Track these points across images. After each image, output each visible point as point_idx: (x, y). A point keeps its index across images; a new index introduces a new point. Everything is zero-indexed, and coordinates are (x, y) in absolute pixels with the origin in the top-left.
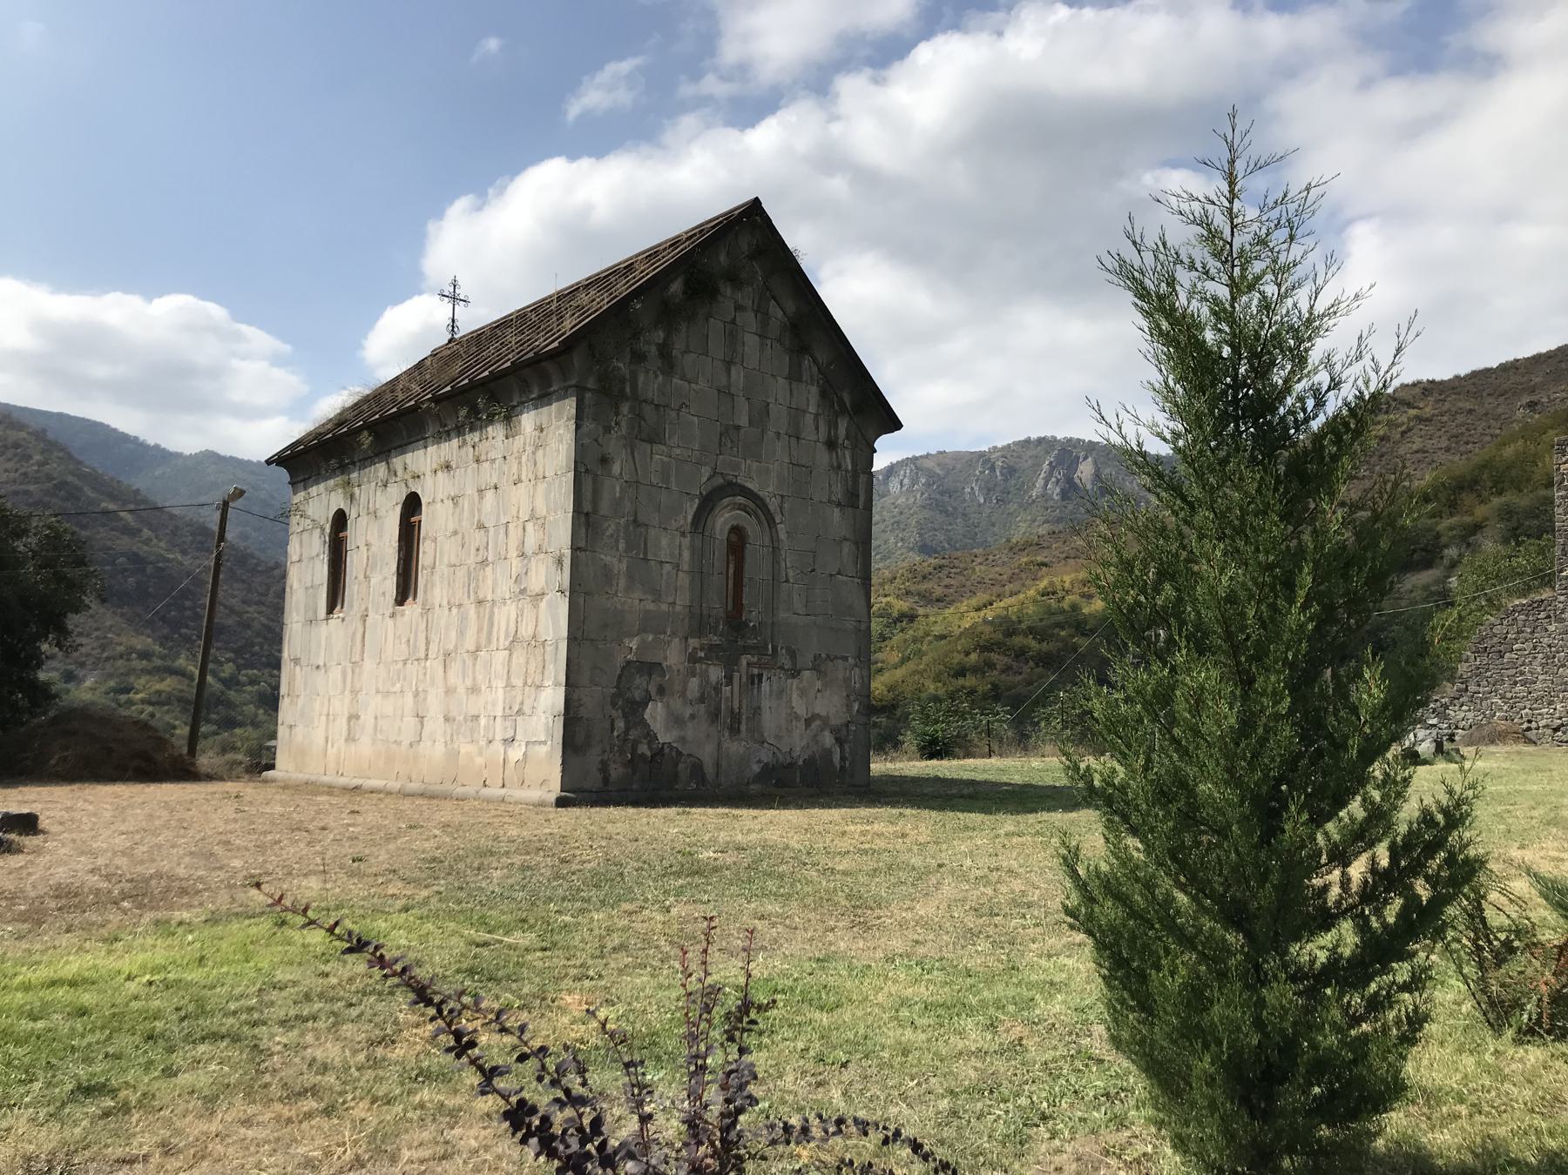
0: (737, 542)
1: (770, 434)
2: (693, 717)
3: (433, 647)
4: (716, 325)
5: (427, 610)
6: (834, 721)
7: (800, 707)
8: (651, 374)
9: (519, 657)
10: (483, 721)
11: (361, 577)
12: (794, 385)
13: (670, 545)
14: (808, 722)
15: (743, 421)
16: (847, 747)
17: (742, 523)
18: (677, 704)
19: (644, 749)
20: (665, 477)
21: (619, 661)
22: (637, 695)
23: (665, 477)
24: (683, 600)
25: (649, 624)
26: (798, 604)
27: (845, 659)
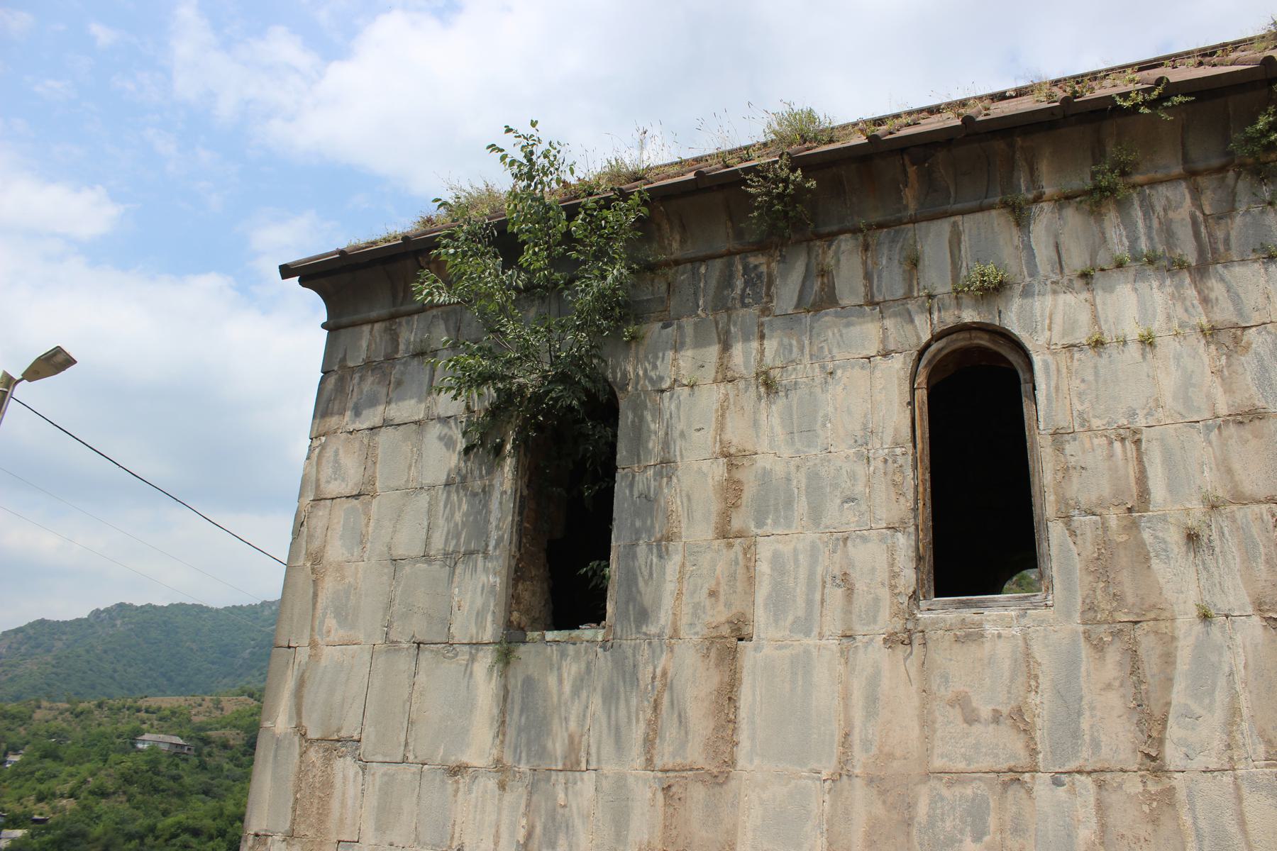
3: (1192, 739)
5: (1125, 627)
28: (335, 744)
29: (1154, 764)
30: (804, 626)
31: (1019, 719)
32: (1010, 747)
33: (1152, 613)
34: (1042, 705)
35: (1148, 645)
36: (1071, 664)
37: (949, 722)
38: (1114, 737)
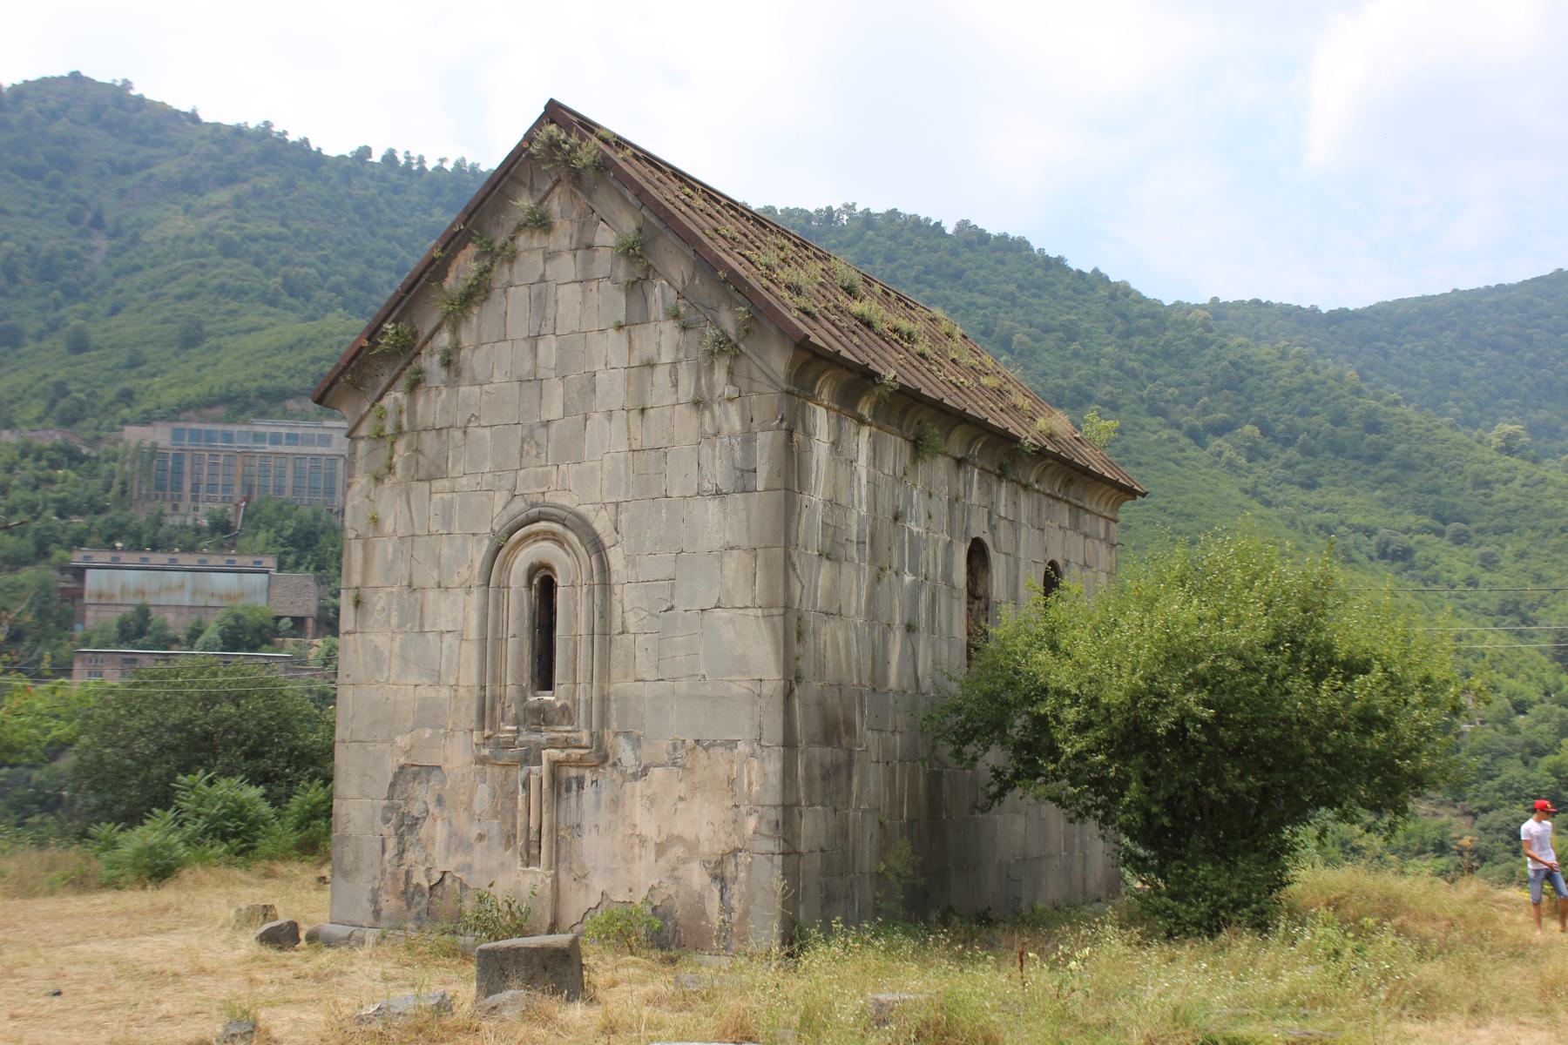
0: (544, 586)
1: (597, 418)
2: (481, 837)
4: (519, 294)
6: (705, 848)
7: (647, 826)
8: (433, 393)
12: (637, 332)
13: (457, 612)
14: (661, 849)
15: (554, 409)
16: (736, 890)
17: (547, 559)
18: (461, 819)
19: (419, 878)
20: (447, 519)
21: (391, 766)
22: (416, 809)
23: (447, 519)
24: (470, 676)
25: (428, 715)
26: (644, 668)
27: (731, 744)
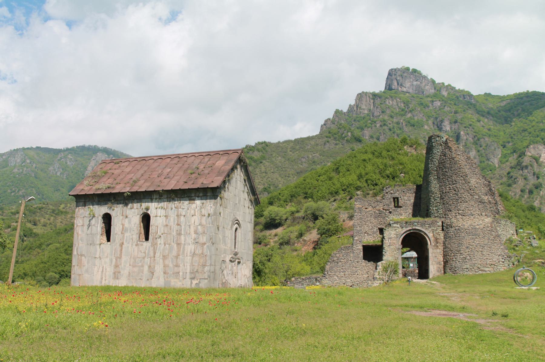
3: (157, 255)
5: (154, 245)
9: (196, 258)
10: (181, 274)
11: (120, 233)
28: (82, 255)
29: (154, 257)
30: (128, 243)
31: (145, 253)
32: (144, 255)
33: (156, 244)
34: (147, 251)
35: (156, 246)
36: (149, 248)
37: (140, 253)
38: (152, 254)
